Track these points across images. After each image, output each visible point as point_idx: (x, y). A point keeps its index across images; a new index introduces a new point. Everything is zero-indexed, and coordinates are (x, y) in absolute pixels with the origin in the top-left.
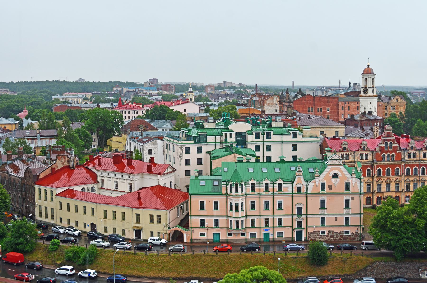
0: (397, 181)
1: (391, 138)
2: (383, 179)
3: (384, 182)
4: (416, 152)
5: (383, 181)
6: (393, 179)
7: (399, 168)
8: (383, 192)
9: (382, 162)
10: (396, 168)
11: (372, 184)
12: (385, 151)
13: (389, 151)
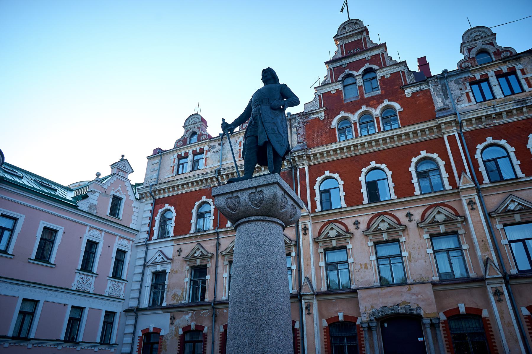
0: (434, 223)
1: (367, 55)
2: (350, 223)
3: (358, 234)
4: (518, 67)
5: (352, 228)
6: (409, 215)
7: (435, 156)
8: (355, 291)
9: (334, 146)
10: (414, 160)
11: (293, 254)
12: (348, 104)
13: (368, 102)
